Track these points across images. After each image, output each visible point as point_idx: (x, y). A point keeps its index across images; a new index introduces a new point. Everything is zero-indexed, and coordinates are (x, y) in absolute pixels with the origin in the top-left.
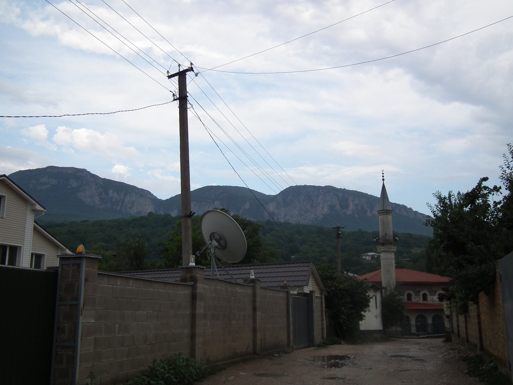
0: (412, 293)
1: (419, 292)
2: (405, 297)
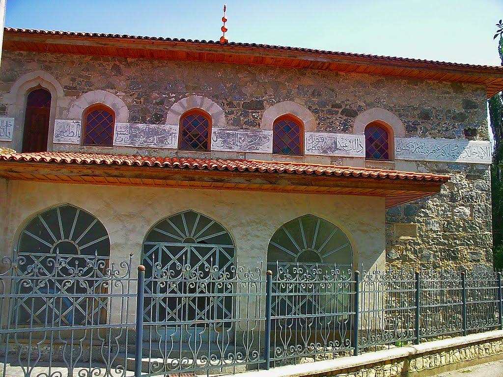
0: (213, 108)
1: (259, 106)
2: (172, 127)
